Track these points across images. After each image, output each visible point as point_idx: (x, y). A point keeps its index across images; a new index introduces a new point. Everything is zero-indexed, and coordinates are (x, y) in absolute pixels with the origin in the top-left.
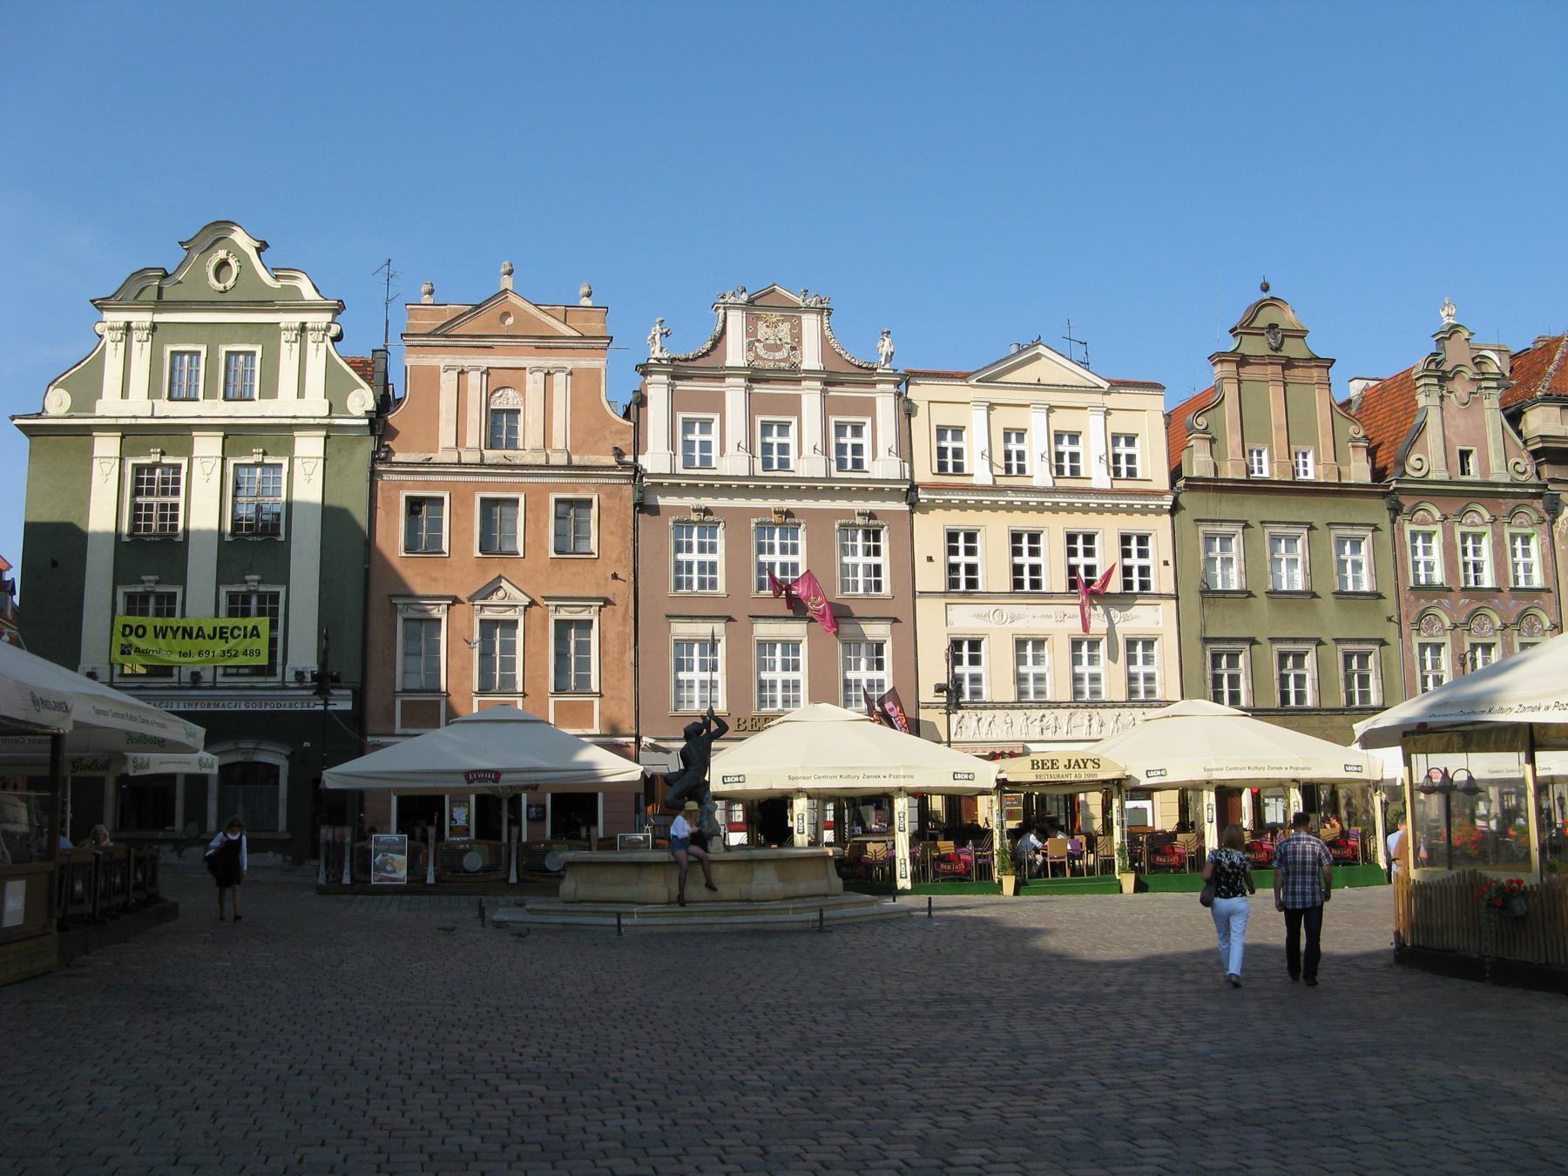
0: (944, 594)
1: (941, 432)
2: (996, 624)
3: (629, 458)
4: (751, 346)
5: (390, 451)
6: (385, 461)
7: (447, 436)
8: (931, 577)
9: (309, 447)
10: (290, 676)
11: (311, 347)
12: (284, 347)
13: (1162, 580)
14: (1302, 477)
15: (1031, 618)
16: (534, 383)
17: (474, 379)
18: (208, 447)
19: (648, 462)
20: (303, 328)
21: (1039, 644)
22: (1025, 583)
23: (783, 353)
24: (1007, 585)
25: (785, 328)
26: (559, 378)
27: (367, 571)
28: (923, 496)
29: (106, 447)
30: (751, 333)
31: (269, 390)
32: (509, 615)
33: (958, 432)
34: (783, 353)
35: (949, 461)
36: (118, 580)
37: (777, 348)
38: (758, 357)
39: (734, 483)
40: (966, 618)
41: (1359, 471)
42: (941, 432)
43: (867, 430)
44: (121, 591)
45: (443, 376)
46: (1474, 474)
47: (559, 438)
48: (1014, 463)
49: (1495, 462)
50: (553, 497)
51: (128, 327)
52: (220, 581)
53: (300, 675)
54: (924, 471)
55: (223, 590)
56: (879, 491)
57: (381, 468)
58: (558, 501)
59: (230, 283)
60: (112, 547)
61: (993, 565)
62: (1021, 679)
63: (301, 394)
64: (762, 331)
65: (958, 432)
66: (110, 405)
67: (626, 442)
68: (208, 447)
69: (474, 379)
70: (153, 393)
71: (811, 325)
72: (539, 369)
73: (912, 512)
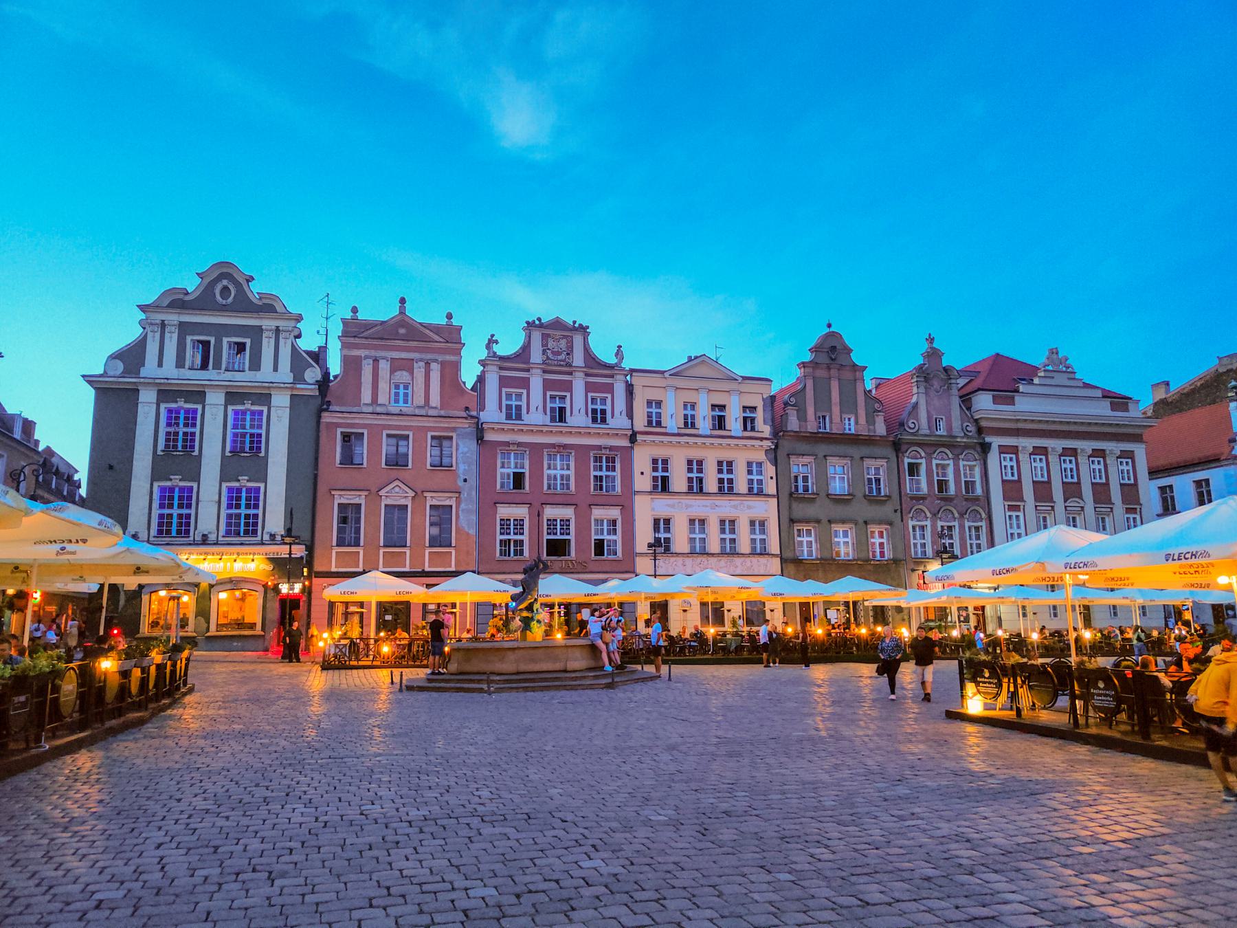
0: (650, 493)
1: (649, 403)
2: (680, 510)
3: (474, 413)
4: (544, 352)
5: (329, 403)
6: (327, 410)
7: (366, 397)
8: (642, 482)
9: (281, 400)
10: (266, 537)
11: (282, 342)
12: (265, 341)
13: (771, 488)
14: (847, 431)
15: (698, 506)
17: (384, 366)
18: (215, 399)
19: (484, 416)
20: (277, 330)
21: (702, 522)
22: (696, 487)
23: (563, 356)
24: (684, 488)
25: (563, 343)
26: (435, 368)
27: (316, 476)
28: (639, 437)
29: (147, 397)
30: (545, 345)
31: (256, 365)
32: (403, 502)
33: (659, 404)
34: (563, 356)
35: (655, 422)
36: (155, 477)
37: (559, 353)
38: (548, 358)
39: (535, 429)
40: (662, 506)
41: (881, 429)
42: (649, 403)
43: (609, 402)
44: (156, 485)
45: (364, 362)
46: (942, 432)
47: (435, 400)
48: (689, 422)
49: (956, 424)
50: (429, 434)
51: (163, 325)
52: (222, 480)
53: (273, 536)
54: (640, 423)
55: (224, 485)
57: (324, 414)
58: (433, 438)
59: (230, 300)
60: (150, 458)
62: (692, 540)
63: (276, 369)
64: (551, 344)
66: (150, 368)
68: (215, 399)
69: (384, 366)
70: (180, 363)
71: (578, 340)
72: (421, 360)
73: (632, 448)
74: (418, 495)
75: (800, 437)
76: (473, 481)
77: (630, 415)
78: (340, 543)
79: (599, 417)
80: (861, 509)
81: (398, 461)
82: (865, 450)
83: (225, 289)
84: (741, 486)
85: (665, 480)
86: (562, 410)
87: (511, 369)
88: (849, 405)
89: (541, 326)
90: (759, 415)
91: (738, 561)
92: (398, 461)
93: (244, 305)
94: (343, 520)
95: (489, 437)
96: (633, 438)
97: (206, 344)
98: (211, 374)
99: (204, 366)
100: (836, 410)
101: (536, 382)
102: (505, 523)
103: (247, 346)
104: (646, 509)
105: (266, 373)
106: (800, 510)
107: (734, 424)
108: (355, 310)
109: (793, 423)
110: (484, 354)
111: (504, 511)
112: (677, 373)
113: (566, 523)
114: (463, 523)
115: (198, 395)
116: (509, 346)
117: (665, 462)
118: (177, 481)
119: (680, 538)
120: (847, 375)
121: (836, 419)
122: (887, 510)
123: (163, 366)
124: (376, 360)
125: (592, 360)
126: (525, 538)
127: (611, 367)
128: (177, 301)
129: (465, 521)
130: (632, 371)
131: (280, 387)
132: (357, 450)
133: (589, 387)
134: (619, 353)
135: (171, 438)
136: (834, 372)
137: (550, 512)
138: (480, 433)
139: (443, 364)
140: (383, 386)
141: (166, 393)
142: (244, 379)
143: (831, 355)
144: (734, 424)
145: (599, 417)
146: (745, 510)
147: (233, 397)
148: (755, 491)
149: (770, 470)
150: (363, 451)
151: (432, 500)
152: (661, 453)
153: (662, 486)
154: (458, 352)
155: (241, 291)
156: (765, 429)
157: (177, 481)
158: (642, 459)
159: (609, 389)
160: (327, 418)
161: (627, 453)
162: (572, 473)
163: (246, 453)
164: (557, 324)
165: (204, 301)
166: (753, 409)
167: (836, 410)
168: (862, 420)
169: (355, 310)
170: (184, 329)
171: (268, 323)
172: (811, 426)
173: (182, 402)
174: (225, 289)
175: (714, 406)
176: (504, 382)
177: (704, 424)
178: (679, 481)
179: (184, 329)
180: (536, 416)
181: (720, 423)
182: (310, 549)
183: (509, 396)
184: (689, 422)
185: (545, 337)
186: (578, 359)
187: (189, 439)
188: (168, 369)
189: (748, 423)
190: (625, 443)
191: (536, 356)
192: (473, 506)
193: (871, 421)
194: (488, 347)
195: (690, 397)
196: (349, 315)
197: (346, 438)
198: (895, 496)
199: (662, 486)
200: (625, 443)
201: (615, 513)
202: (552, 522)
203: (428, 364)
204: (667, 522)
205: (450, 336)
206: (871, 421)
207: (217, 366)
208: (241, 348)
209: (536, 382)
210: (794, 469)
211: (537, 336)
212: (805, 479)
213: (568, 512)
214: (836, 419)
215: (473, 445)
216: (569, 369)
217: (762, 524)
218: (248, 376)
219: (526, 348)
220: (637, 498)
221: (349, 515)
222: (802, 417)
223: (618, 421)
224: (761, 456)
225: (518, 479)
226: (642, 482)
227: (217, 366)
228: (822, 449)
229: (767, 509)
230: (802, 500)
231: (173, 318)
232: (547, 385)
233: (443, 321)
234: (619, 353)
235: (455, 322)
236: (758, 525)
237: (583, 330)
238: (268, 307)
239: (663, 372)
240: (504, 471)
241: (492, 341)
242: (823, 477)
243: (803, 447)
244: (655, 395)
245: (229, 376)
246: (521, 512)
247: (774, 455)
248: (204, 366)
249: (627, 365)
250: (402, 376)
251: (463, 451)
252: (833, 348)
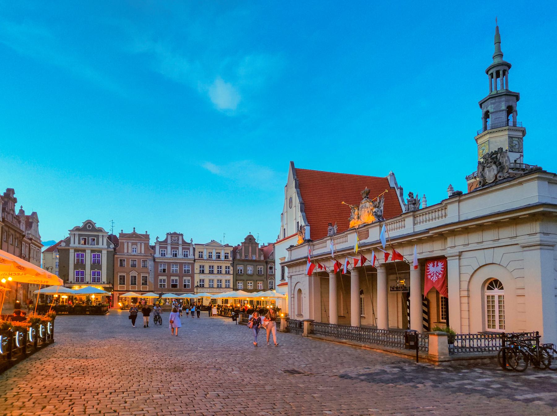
1: (199, 252)
2: (207, 278)
7: (126, 251)
8: (197, 270)
9: (104, 252)
13: (231, 272)
16: (139, 245)
17: (130, 244)
18: (88, 252)
19: (155, 256)
22: (211, 272)
24: (208, 272)
29: (72, 251)
30: (171, 238)
31: (98, 244)
33: (202, 252)
35: (201, 256)
40: (202, 277)
41: (262, 258)
42: (199, 252)
47: (143, 252)
48: (210, 257)
51: (74, 234)
54: (197, 257)
56: (190, 259)
61: (207, 270)
64: (173, 238)
65: (202, 252)
66: (72, 244)
67: (152, 253)
68: (88, 252)
69: (130, 244)
70: (79, 243)
71: (180, 237)
74: (139, 274)
75: (239, 260)
76: (153, 270)
77: (194, 255)
78: (120, 284)
79: (186, 256)
80: (255, 277)
81: (134, 266)
82: (257, 263)
83: (89, 226)
84: (224, 272)
85: (203, 270)
86: (176, 254)
87: (163, 244)
88: (254, 252)
89: (171, 234)
90: (229, 255)
91: (222, 289)
92: (134, 266)
93: (94, 229)
94: (120, 279)
95: (157, 260)
96: (194, 261)
97: (85, 239)
98: (87, 246)
99: (85, 244)
100: (250, 254)
101: (169, 248)
102: (161, 281)
103: (95, 239)
104: (197, 278)
105: (100, 246)
106: (239, 278)
107: (222, 257)
108: (122, 231)
109: (238, 257)
110: (155, 241)
111: (160, 278)
112: (207, 245)
113: (176, 280)
114: (150, 280)
115: (84, 251)
116: (162, 239)
117: (203, 266)
118: (80, 270)
119: (206, 284)
120: (254, 245)
121: (250, 256)
122: (263, 278)
123: (75, 244)
124: (128, 243)
125: (184, 242)
126: (166, 284)
127: (189, 244)
128: (77, 229)
129: (151, 279)
130: (195, 244)
131: (104, 249)
132: (123, 263)
133: (183, 249)
134: (192, 240)
135: (78, 260)
136: (250, 245)
137: (172, 278)
138: (154, 260)
139: (145, 244)
140: (130, 248)
141: (76, 250)
142: (95, 247)
143: (250, 240)
144: (222, 257)
145: (186, 256)
146: (224, 278)
147: (92, 251)
148: (227, 273)
149: (231, 268)
150: (125, 263)
151: (142, 275)
152: (202, 264)
153: (202, 272)
154: (149, 241)
155: (93, 226)
156: (231, 259)
157: (80, 270)
158: (197, 266)
159: (189, 249)
160: (116, 256)
161: (193, 265)
162: (178, 269)
163: (96, 265)
164: (175, 233)
165: (84, 228)
166: (228, 253)
167: (250, 254)
168: (257, 256)
169: (122, 231)
170: (80, 235)
171: (100, 234)
172: (243, 258)
173: (80, 252)
174: (89, 226)
175: (217, 253)
176: (160, 247)
177: (214, 257)
178: (207, 270)
179: (80, 235)
180: (169, 255)
181: (219, 257)
182: (113, 285)
183: (162, 251)
184: (210, 257)
185: (171, 237)
186: (180, 242)
187: (82, 261)
188: (76, 245)
189: (226, 257)
190: (193, 262)
191: (169, 241)
192: (153, 276)
193: (260, 256)
194: (157, 239)
195: (211, 251)
196: (121, 232)
197: (121, 260)
198: (265, 274)
199: (202, 272)
200: (193, 262)
201: (189, 278)
202: (173, 280)
203: (141, 243)
204: (203, 280)
205: (147, 237)
206: (260, 256)
207: (88, 244)
208: (94, 240)
209: (169, 248)
210: (238, 268)
211: (169, 237)
212: (241, 270)
213: (177, 278)
214: (250, 256)
215: (153, 262)
216: (178, 244)
217: (229, 281)
218: (96, 246)
219: (166, 239)
220: (195, 275)
221: (122, 279)
222: (241, 255)
223: (191, 256)
224: (229, 265)
225: (164, 270)
226: (197, 270)
227: (88, 244)
228: (246, 263)
229: (230, 277)
230: (240, 275)
231: (77, 233)
232: (172, 248)
233: (145, 233)
234: (192, 240)
235: (148, 233)
236: (228, 281)
237: (182, 235)
238: (100, 230)
239: (203, 245)
240: (161, 268)
241: (157, 238)
242: (246, 270)
243: (241, 263)
244: (201, 250)
245: (91, 246)
246: (165, 278)
247: (233, 265)
248: (85, 244)
249: (193, 243)
250: (135, 246)
251: (150, 264)
252: (250, 239)
